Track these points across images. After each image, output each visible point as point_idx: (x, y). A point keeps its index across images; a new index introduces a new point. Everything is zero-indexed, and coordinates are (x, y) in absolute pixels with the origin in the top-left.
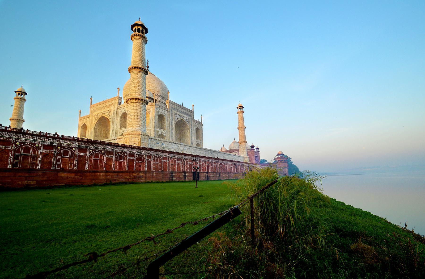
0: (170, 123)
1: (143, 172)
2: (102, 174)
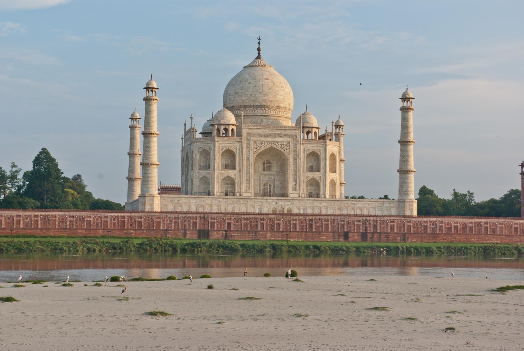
1: (133, 230)
2: (101, 231)
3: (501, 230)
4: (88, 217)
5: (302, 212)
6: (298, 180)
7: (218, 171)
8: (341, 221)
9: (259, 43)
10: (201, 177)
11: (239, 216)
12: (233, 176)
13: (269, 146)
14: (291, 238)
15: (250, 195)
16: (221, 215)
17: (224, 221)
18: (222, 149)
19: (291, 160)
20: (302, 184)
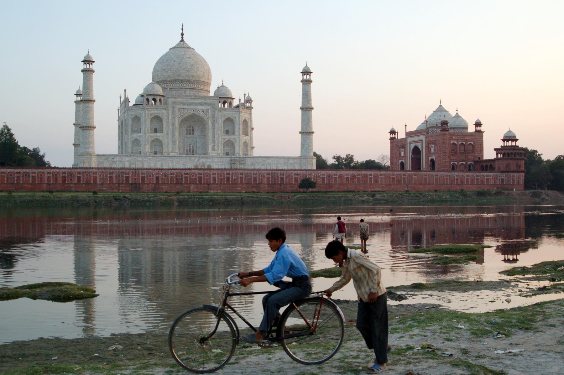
0: (171, 123)
2: (45, 185)
3: (382, 181)
4: (33, 173)
5: (220, 167)
6: (216, 142)
7: (148, 135)
8: (254, 174)
9: (182, 29)
10: (133, 139)
11: (166, 171)
12: (161, 139)
13: (192, 112)
14: (211, 190)
15: (176, 154)
16: (150, 171)
17: (153, 176)
18: (151, 115)
19: (210, 125)
20: (220, 145)
